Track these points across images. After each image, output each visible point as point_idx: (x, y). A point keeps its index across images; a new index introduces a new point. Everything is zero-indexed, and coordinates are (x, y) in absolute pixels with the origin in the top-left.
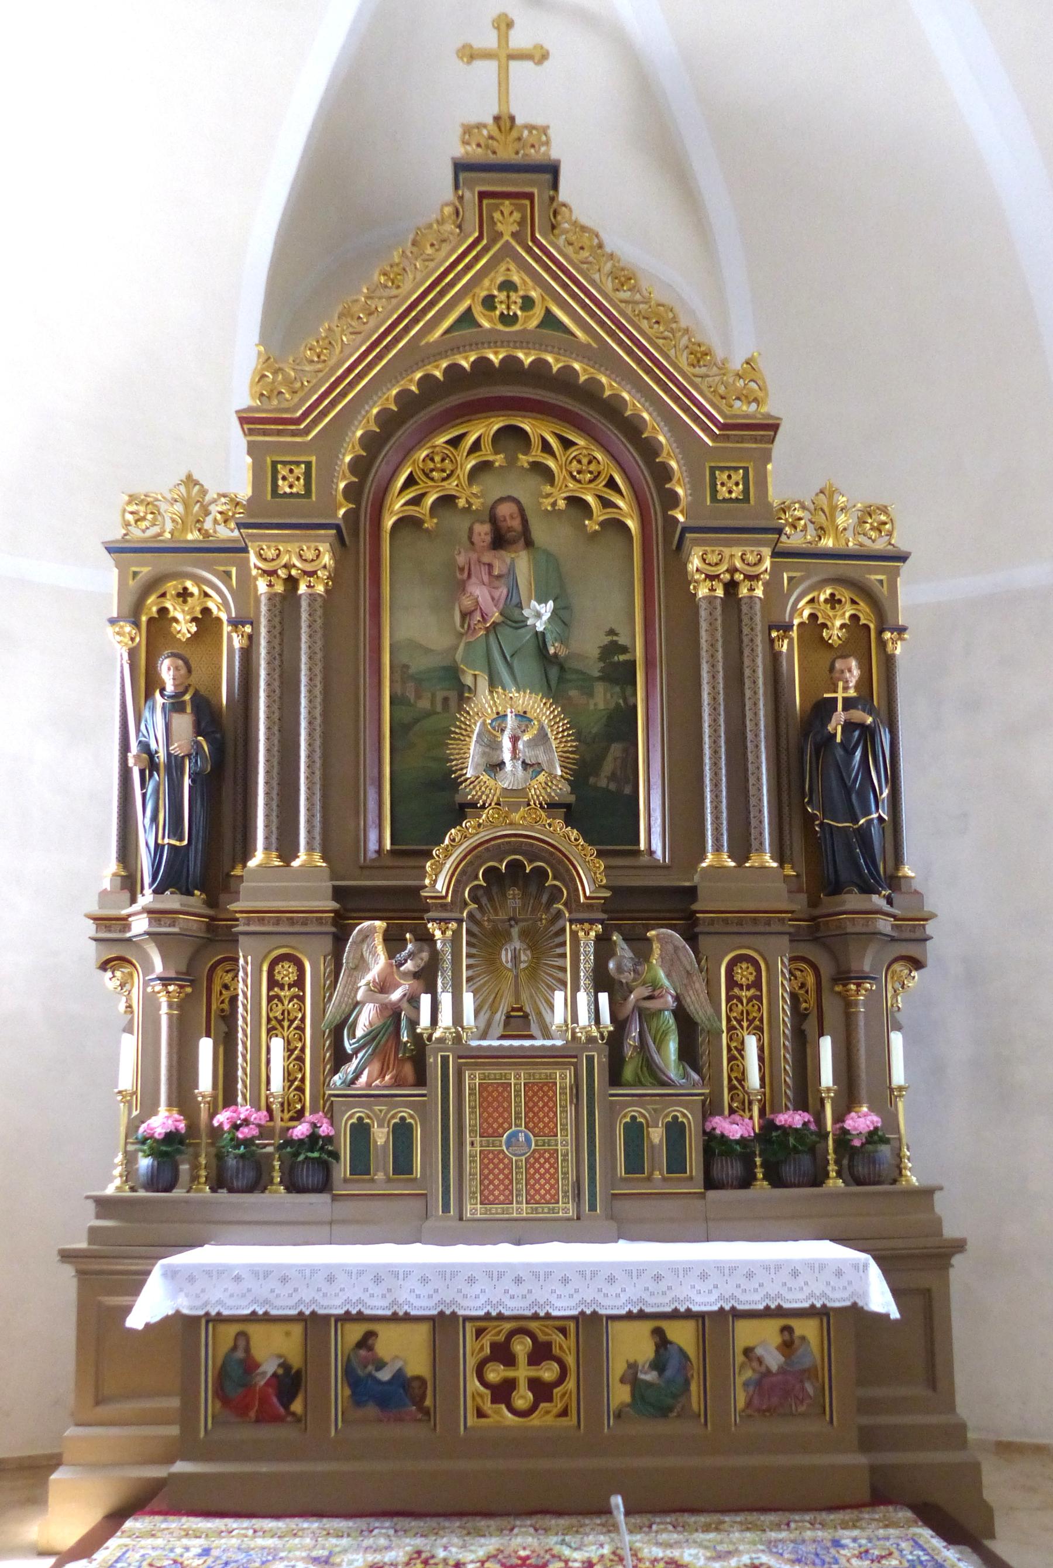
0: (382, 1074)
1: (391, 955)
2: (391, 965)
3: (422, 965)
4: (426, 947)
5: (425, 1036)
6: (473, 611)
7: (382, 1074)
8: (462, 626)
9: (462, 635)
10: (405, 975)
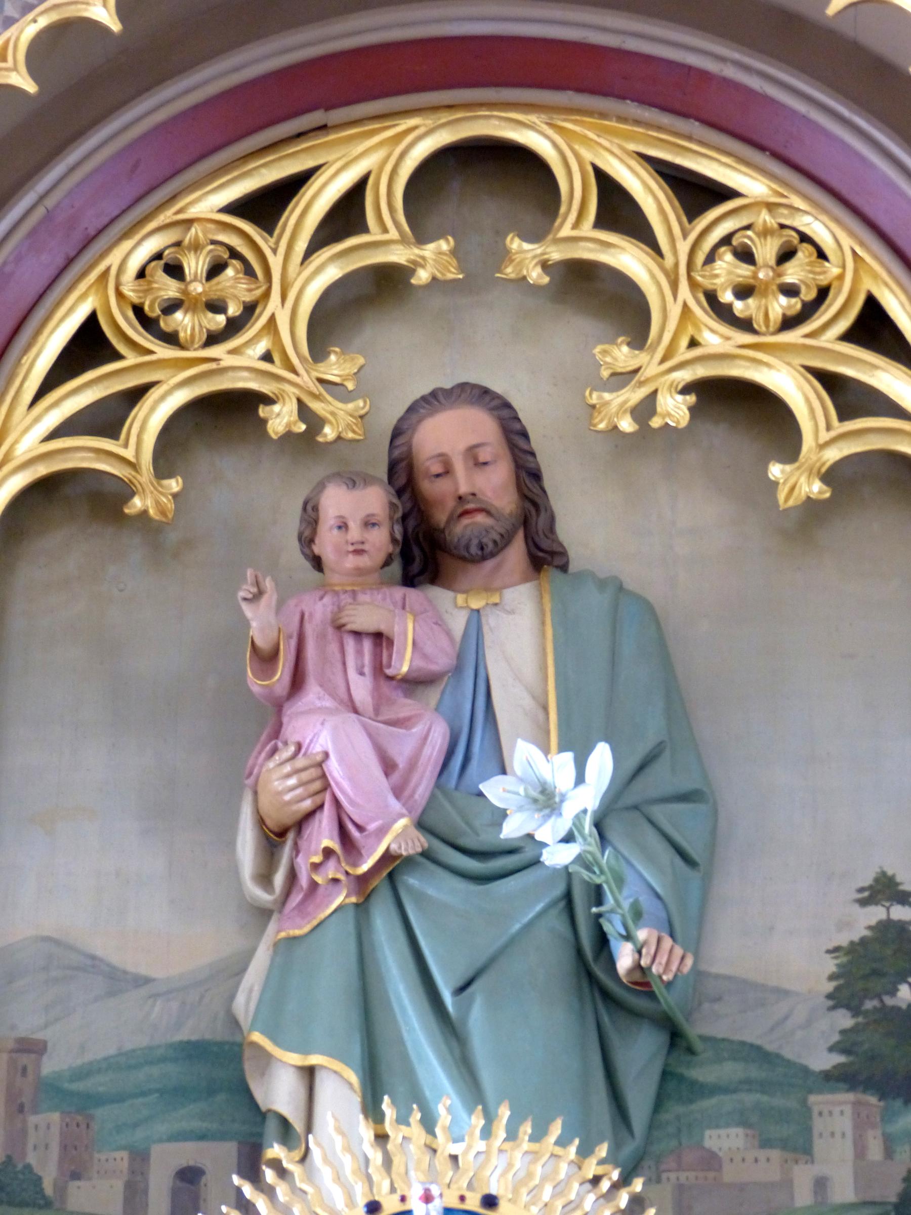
6: (310, 815)
8: (265, 879)
9: (264, 914)
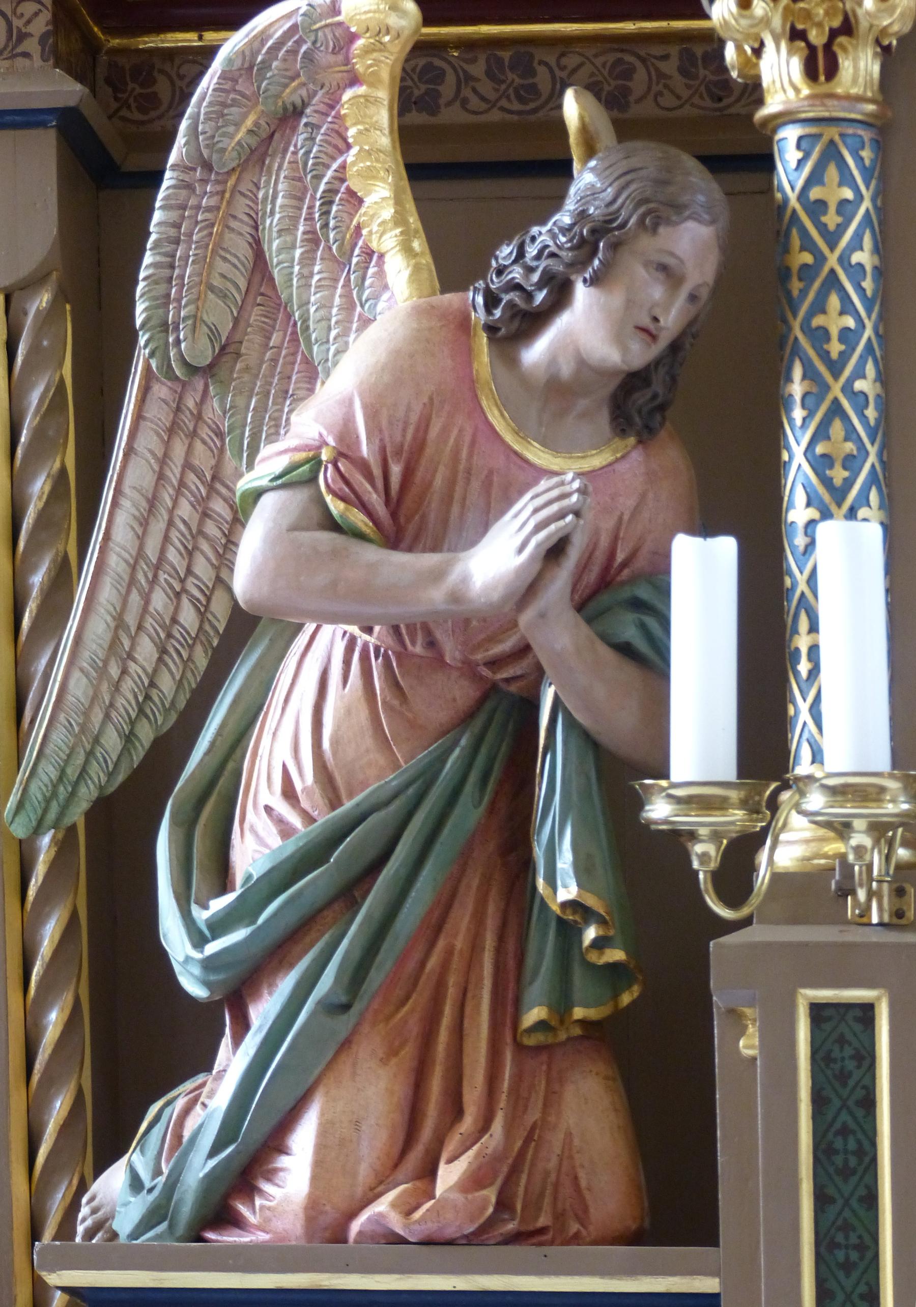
0: (412, 1154)
1: (454, 260)
2: (464, 324)
3: (672, 320)
4: (701, 186)
5: (704, 854)
7: (412, 1154)
10: (556, 394)
